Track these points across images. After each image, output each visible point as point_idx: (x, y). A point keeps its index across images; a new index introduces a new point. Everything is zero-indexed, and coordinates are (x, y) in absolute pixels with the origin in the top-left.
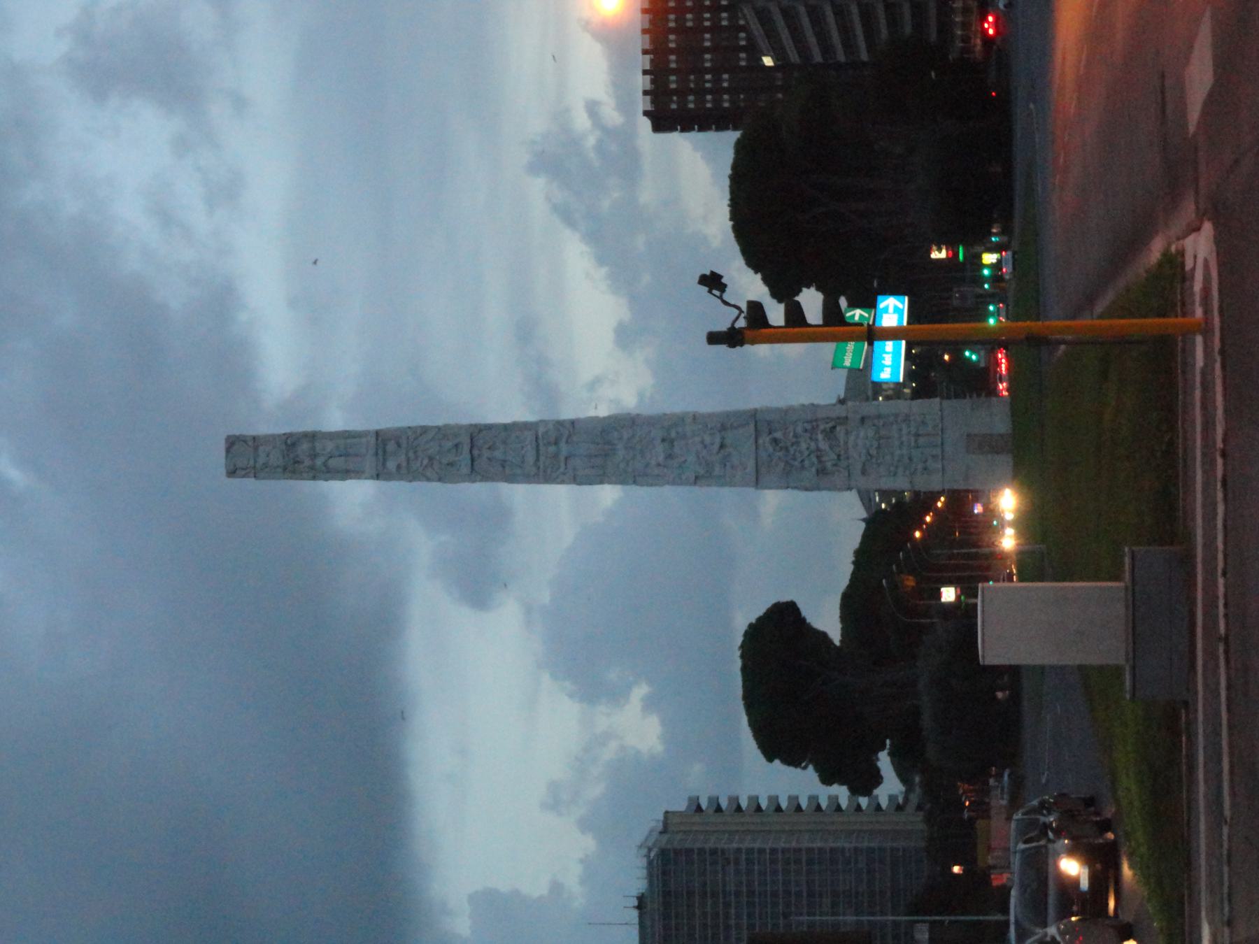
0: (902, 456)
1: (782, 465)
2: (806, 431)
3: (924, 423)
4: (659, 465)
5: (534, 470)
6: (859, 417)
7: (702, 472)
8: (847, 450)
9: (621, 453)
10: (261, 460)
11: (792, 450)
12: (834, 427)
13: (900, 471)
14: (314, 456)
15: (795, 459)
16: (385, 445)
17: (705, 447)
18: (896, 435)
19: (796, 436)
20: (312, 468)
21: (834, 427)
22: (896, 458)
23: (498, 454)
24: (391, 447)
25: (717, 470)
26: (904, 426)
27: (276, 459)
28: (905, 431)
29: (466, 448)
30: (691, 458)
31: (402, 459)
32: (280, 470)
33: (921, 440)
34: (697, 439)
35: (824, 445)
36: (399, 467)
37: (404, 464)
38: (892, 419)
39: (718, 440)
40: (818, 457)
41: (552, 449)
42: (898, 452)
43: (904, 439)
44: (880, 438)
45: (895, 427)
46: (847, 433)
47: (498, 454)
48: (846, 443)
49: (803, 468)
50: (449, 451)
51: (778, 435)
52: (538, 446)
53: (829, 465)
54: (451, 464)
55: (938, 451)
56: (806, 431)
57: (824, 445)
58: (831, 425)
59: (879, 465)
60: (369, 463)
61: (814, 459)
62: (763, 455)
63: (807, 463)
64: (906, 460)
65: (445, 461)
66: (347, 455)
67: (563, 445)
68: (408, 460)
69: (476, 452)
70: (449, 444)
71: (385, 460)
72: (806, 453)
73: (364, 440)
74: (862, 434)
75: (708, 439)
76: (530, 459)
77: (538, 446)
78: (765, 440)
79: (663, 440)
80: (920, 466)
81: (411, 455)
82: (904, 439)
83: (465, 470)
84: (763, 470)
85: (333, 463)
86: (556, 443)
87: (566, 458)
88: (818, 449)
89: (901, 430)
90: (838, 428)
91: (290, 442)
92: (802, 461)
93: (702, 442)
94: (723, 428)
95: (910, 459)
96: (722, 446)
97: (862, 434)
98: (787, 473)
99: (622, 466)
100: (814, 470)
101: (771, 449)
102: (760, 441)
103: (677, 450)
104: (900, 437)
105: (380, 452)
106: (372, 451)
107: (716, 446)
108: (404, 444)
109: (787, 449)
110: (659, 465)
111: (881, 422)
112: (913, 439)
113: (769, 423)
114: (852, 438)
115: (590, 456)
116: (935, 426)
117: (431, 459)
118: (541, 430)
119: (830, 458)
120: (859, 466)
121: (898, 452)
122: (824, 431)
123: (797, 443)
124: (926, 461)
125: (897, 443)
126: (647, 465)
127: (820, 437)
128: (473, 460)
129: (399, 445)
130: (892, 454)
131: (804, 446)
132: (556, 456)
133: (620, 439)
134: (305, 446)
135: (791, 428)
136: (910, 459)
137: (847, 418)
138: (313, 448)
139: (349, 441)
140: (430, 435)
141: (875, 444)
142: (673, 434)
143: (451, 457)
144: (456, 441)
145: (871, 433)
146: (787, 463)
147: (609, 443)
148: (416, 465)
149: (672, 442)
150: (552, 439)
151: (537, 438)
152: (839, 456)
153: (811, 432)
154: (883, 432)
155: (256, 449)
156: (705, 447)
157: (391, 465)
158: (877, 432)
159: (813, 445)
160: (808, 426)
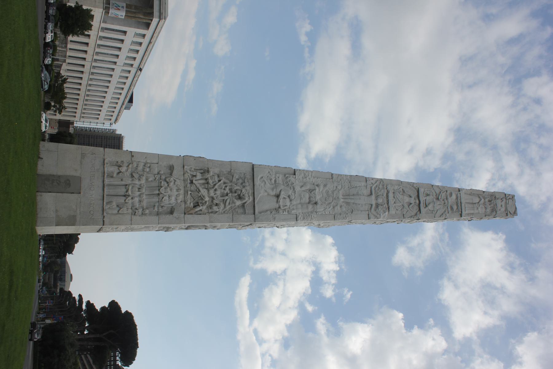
0: (139, 180)
1: (234, 180)
2: (217, 205)
3: (119, 207)
4: (318, 186)
5: (389, 187)
6: (175, 214)
7: (292, 178)
8: (185, 187)
9: (341, 196)
10: (503, 203)
11: (227, 190)
12: (195, 207)
13: (140, 168)
14: (484, 204)
15: (225, 183)
16: (457, 208)
17: (289, 196)
18: (144, 197)
19: (224, 202)
20: (485, 198)
21: (195, 207)
22: (144, 178)
23: (407, 199)
24: (455, 207)
25: (281, 177)
26: (137, 205)
27: (499, 202)
28: (137, 199)
29: (422, 205)
30: (298, 189)
31: (450, 200)
32: (497, 197)
33: (122, 191)
34: (294, 202)
35: (204, 192)
36: (451, 195)
37: (448, 197)
38: (147, 211)
39: (281, 200)
40: (208, 183)
41: (380, 201)
42: (143, 181)
43: (138, 193)
44: (159, 194)
45: (145, 204)
46: (185, 202)
47: (407, 199)
48: (186, 192)
49: (218, 176)
50: (429, 204)
51: (239, 203)
52: (388, 204)
53: (199, 176)
54: (428, 195)
55: (107, 181)
56: (217, 205)
57: (204, 192)
58: (198, 209)
59: (158, 173)
60: (465, 199)
61: (211, 181)
62: (249, 188)
63: (217, 179)
64: (136, 176)
65: (431, 197)
66: (473, 203)
67: (374, 203)
68: (447, 199)
69: (418, 202)
70: (430, 207)
71: (457, 198)
72: (216, 187)
73: (467, 212)
74: (173, 198)
75: (288, 203)
76: (391, 195)
77: (388, 204)
78: (248, 200)
79: (316, 203)
80: (123, 169)
81: (446, 202)
82: (138, 193)
83: (421, 190)
84: (249, 176)
85: (477, 200)
86: (377, 206)
87: (371, 194)
88: (208, 189)
89: (140, 201)
90: (192, 205)
91: (493, 212)
92: (220, 181)
93: (291, 200)
94: (277, 210)
95: (132, 176)
96: (278, 196)
97: (173, 198)
98: (231, 173)
99: (339, 187)
100: (211, 174)
101: (243, 191)
102: (251, 198)
103: (307, 196)
104: (140, 196)
105: (459, 204)
106: (463, 205)
107: (282, 196)
108: (449, 209)
109: (231, 190)
110: (318, 186)
111: (156, 209)
112: (130, 192)
113: (245, 213)
114: (181, 198)
115: (358, 194)
116: (109, 203)
117: (438, 199)
118: (387, 213)
119: (199, 181)
120: (175, 172)
121: (143, 181)
122: (203, 204)
123: (222, 196)
124: (118, 173)
125: (143, 190)
126: (325, 186)
127: (207, 199)
128: (418, 196)
129: (452, 208)
130: (147, 179)
131: (218, 192)
132: (377, 197)
133: (341, 207)
134: (489, 210)
135: (228, 207)
136: (132, 176)
137: (185, 214)
138: (486, 208)
139: (472, 212)
140: (439, 213)
141: (162, 190)
142: (310, 206)
143: (428, 198)
144: (427, 208)
145: (166, 200)
146: (231, 181)
147: (348, 203)
148: (443, 195)
149: (309, 203)
150: (380, 207)
151: (389, 209)
152: (192, 182)
153: (213, 203)
154: (156, 199)
155: (506, 209)
156: (289, 196)
157: (454, 197)
158: (160, 201)
159: (212, 192)
160: (215, 208)
